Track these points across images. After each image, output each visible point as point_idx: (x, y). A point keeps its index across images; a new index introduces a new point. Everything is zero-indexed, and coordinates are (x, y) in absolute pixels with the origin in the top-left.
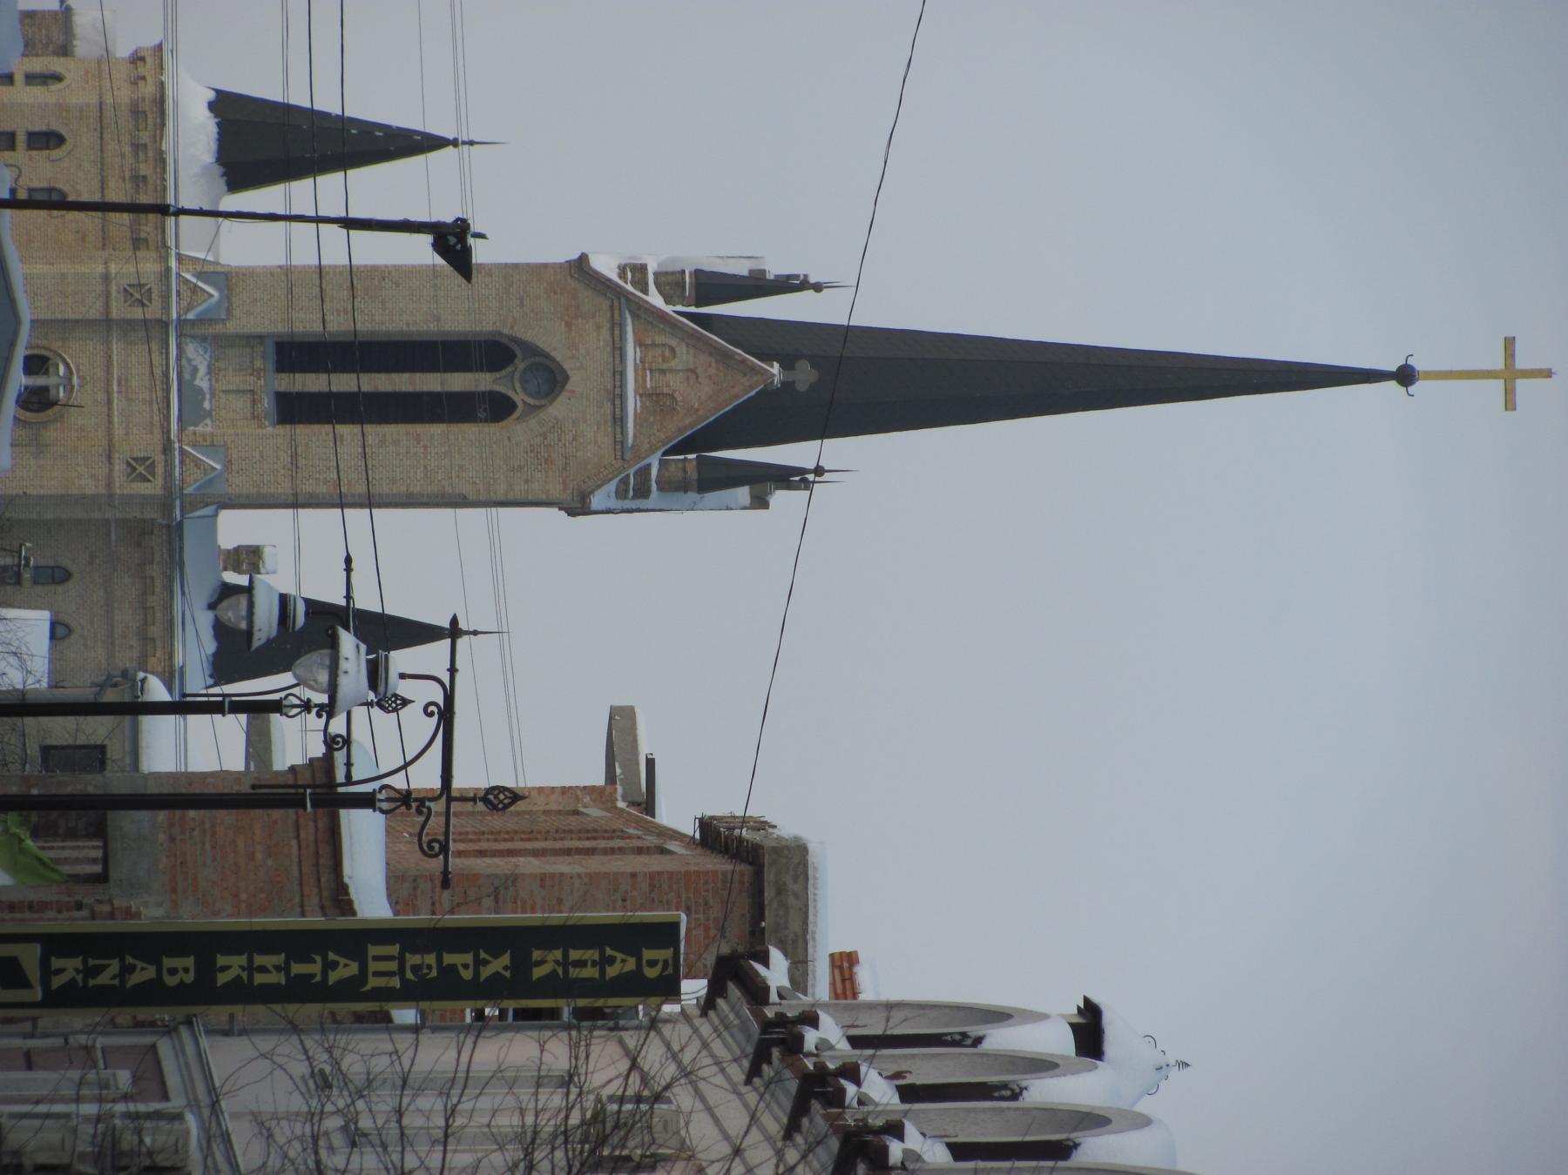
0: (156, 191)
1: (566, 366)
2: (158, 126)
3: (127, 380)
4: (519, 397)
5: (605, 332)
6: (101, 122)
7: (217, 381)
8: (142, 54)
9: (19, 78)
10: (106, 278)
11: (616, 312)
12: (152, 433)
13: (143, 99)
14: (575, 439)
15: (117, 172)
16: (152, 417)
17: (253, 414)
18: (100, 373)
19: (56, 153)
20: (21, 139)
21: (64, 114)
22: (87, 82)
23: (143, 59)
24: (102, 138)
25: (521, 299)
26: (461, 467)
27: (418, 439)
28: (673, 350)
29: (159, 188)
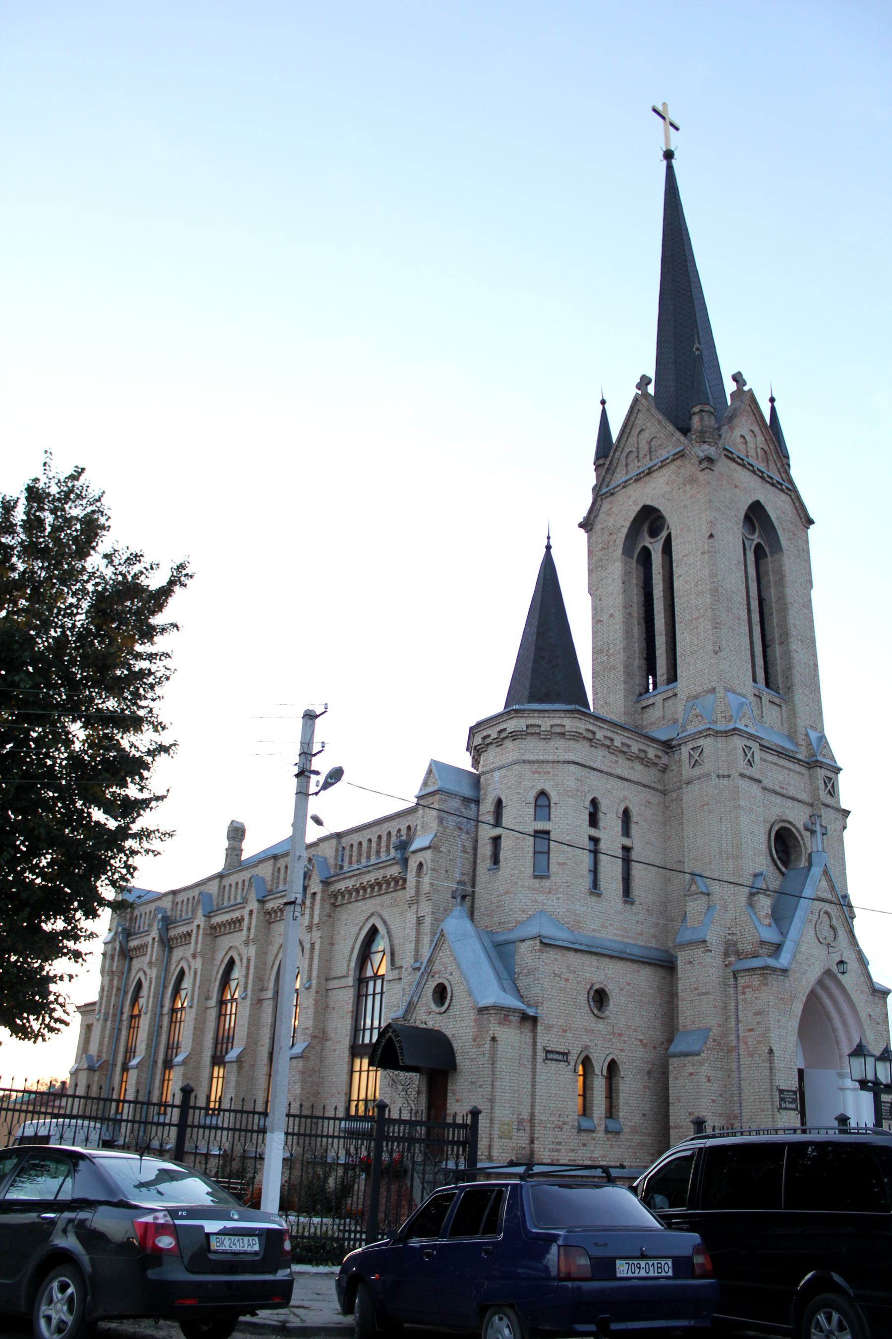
0: (630, 738)
1: (754, 499)
2: (595, 723)
3: (781, 783)
4: (756, 539)
5: (739, 468)
6: (585, 766)
7: (766, 723)
8: (480, 740)
9: (541, 826)
10: (742, 775)
11: (730, 455)
12: (803, 775)
13: (578, 728)
14: (784, 513)
15: (613, 765)
16: (796, 772)
17: (777, 705)
18: (778, 800)
19: (603, 807)
20: (593, 832)
21: (579, 793)
22: (549, 773)
23: (528, 726)
24: (594, 769)
25: (727, 507)
26: (801, 585)
27: (792, 604)
28: (742, 437)
29: (630, 736)
